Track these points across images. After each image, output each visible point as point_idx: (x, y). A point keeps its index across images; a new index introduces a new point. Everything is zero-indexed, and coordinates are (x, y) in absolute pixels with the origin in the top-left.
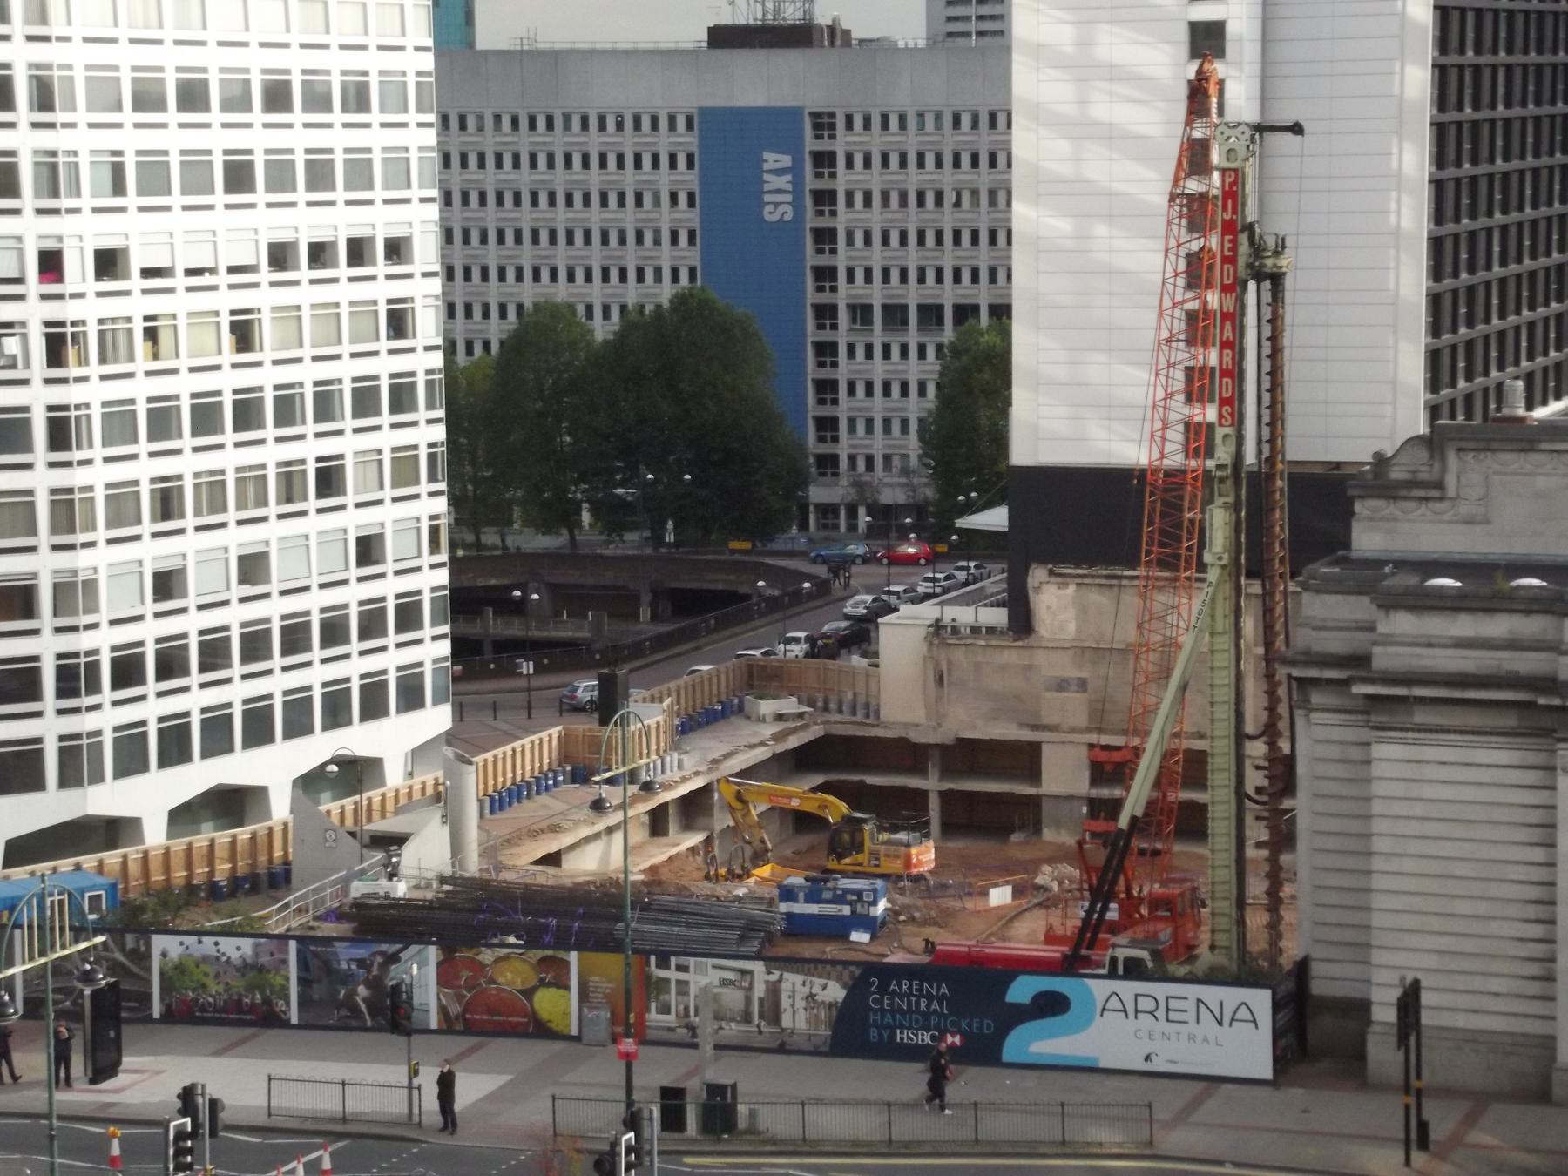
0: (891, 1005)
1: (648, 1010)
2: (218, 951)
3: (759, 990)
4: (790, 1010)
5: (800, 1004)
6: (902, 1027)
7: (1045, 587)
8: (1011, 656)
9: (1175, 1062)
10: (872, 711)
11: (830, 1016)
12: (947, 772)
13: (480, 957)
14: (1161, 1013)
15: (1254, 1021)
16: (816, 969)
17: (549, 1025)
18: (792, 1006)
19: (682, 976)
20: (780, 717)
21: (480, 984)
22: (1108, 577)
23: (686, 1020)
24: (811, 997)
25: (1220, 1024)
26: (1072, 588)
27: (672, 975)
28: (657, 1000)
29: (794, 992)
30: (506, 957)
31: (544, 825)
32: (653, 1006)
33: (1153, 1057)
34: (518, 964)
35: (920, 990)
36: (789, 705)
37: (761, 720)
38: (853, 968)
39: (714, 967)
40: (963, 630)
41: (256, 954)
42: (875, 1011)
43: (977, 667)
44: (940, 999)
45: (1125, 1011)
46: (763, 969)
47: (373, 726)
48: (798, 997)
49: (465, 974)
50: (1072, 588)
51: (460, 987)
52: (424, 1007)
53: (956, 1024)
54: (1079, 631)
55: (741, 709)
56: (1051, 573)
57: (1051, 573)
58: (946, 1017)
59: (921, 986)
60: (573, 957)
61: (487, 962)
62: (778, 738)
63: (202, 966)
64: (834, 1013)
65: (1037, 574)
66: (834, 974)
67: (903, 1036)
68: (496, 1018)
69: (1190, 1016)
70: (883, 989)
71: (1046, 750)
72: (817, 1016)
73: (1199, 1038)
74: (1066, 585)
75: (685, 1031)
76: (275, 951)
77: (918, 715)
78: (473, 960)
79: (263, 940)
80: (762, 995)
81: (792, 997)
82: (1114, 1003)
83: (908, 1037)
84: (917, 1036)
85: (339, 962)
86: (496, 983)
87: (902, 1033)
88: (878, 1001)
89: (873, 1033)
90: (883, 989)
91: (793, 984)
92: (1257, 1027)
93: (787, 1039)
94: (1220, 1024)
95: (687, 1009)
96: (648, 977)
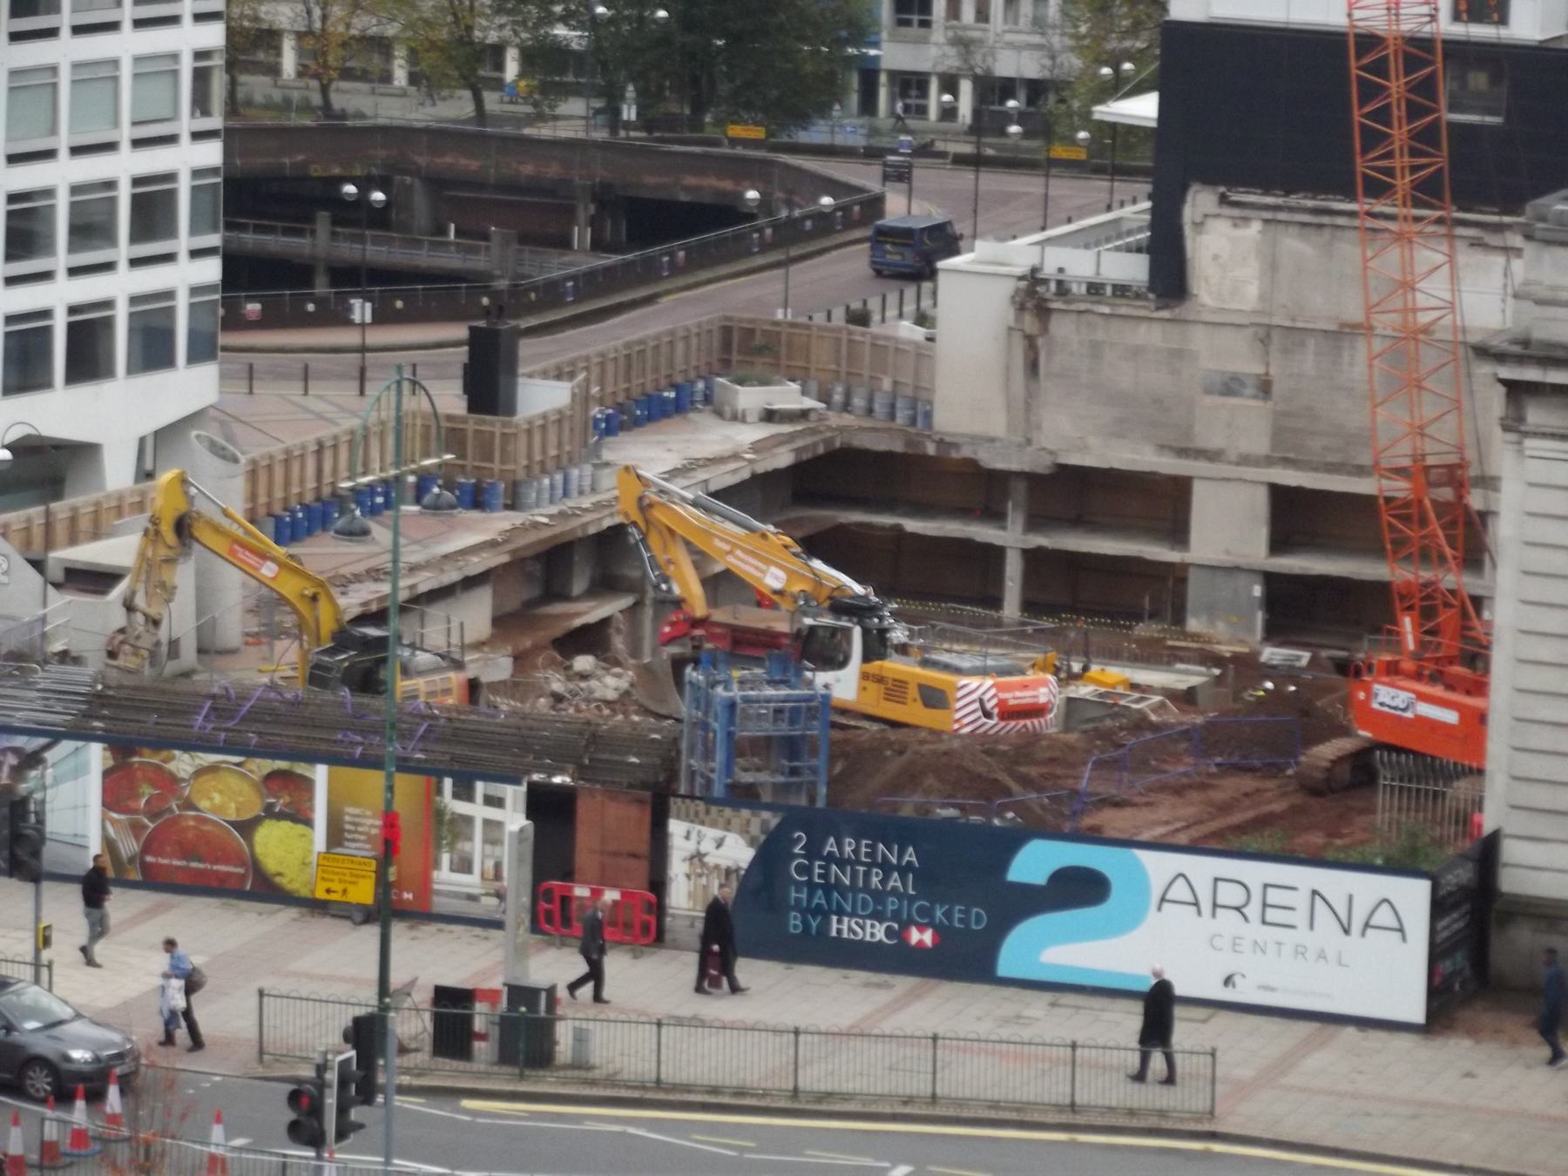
1: (437, 864)
6: (840, 912)
7: (1212, 224)
8: (1152, 334)
9: (1271, 989)
10: (921, 412)
12: (1034, 523)
13: (171, 766)
14: (1253, 910)
15: (1401, 930)
16: (708, 812)
17: (278, 880)
19: (493, 813)
20: (770, 416)
21: (170, 810)
23: (497, 885)
24: (697, 857)
25: (1347, 931)
26: (1255, 227)
27: (477, 810)
30: (213, 769)
31: (360, 568)
32: (445, 858)
33: (1237, 979)
34: (233, 781)
35: (872, 855)
36: (788, 396)
37: (738, 418)
38: (766, 815)
40: (1075, 288)
42: (798, 885)
43: (1096, 349)
44: (904, 870)
45: (1196, 904)
47: (86, 392)
49: (147, 791)
50: (1255, 227)
51: (136, 811)
52: (79, 841)
53: (926, 912)
54: (1262, 297)
55: (708, 399)
56: (1223, 200)
58: (912, 899)
59: (873, 847)
60: (320, 774)
61: (183, 775)
62: (757, 447)
64: (734, 884)
65: (1199, 202)
67: (844, 927)
68: (194, 865)
69: (1299, 918)
71: (1199, 492)
72: (705, 888)
74: (1246, 220)
77: (996, 424)
78: (158, 768)
82: (1180, 891)
83: (850, 930)
84: (863, 928)
86: (196, 809)
87: (839, 922)
88: (805, 870)
89: (794, 922)
90: (813, 851)
92: (1404, 939)
94: (1347, 931)
95: (498, 867)
96: (439, 814)
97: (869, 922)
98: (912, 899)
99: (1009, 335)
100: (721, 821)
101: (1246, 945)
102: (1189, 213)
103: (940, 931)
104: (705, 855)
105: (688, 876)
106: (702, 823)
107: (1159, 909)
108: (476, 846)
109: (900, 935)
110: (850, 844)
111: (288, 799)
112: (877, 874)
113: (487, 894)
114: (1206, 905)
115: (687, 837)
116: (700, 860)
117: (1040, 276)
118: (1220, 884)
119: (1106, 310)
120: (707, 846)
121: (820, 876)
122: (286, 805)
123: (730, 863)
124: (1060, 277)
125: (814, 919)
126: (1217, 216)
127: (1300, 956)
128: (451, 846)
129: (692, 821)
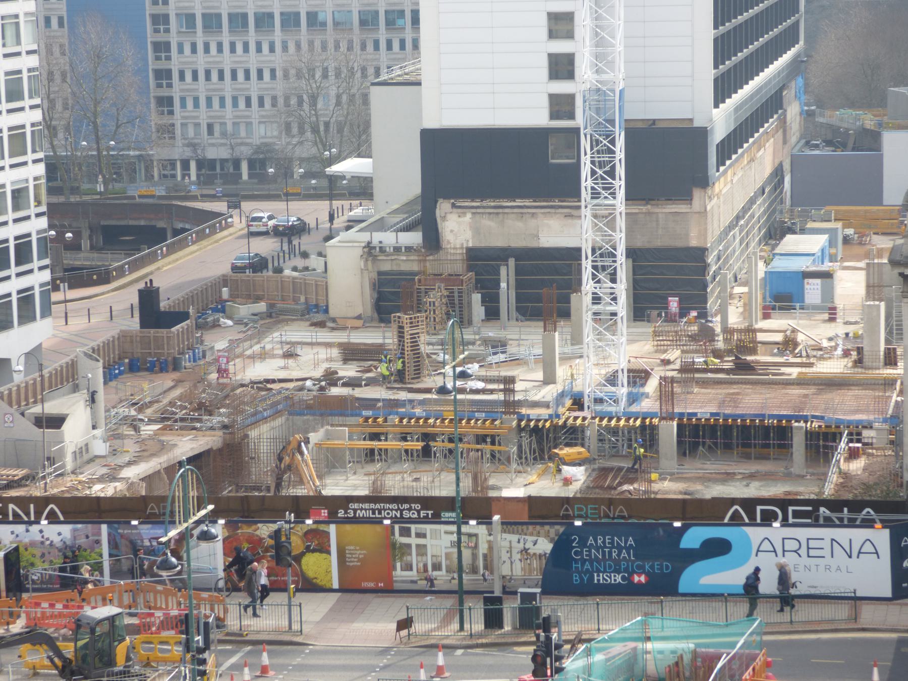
0: (589, 555)
1: (395, 568)
2: (43, 537)
3: (483, 548)
4: (508, 562)
5: (517, 557)
6: (598, 571)
7: (449, 216)
9: (815, 587)
11: (541, 564)
13: (258, 533)
14: (803, 552)
15: (877, 553)
17: (314, 581)
18: (510, 558)
19: (421, 541)
22: (495, 207)
23: (425, 574)
24: (525, 550)
25: (850, 557)
26: (469, 216)
27: (413, 541)
28: (401, 560)
29: (511, 548)
32: (398, 565)
35: (612, 543)
39: (446, 532)
40: (388, 249)
41: (75, 538)
42: (576, 561)
45: (775, 551)
46: (486, 532)
48: (515, 551)
50: (469, 216)
53: (640, 567)
56: (453, 206)
57: (453, 206)
58: (633, 562)
59: (613, 540)
60: (332, 529)
61: (263, 536)
63: (29, 549)
64: (544, 562)
65: (443, 207)
66: (542, 532)
67: (600, 578)
69: (827, 552)
70: (583, 543)
73: (834, 568)
74: (465, 214)
75: (425, 582)
76: (90, 535)
79: (79, 526)
80: (485, 552)
81: (510, 551)
82: (766, 546)
83: (604, 578)
85: (142, 541)
87: (598, 576)
89: (576, 578)
91: (510, 542)
92: (878, 557)
93: (508, 584)
94: (850, 557)
95: (425, 566)
96: (393, 545)
97: (612, 575)
98: (633, 562)
99: (362, 273)
100: (535, 532)
101: (801, 568)
102: (438, 212)
103: (648, 575)
104: (528, 549)
105: (521, 560)
106: (526, 534)
107: (757, 555)
108: (414, 558)
109: (629, 579)
110: (600, 539)
111: (317, 542)
112: (615, 552)
113: (421, 580)
114: (780, 552)
115: (519, 542)
116: (526, 552)
117: (371, 245)
118: (785, 540)
119: (404, 258)
120: (529, 545)
121: (586, 555)
122: (316, 545)
123: (541, 552)
124: (381, 245)
125: (585, 576)
126: (451, 213)
127: (828, 570)
128: (401, 559)
129: (520, 534)
